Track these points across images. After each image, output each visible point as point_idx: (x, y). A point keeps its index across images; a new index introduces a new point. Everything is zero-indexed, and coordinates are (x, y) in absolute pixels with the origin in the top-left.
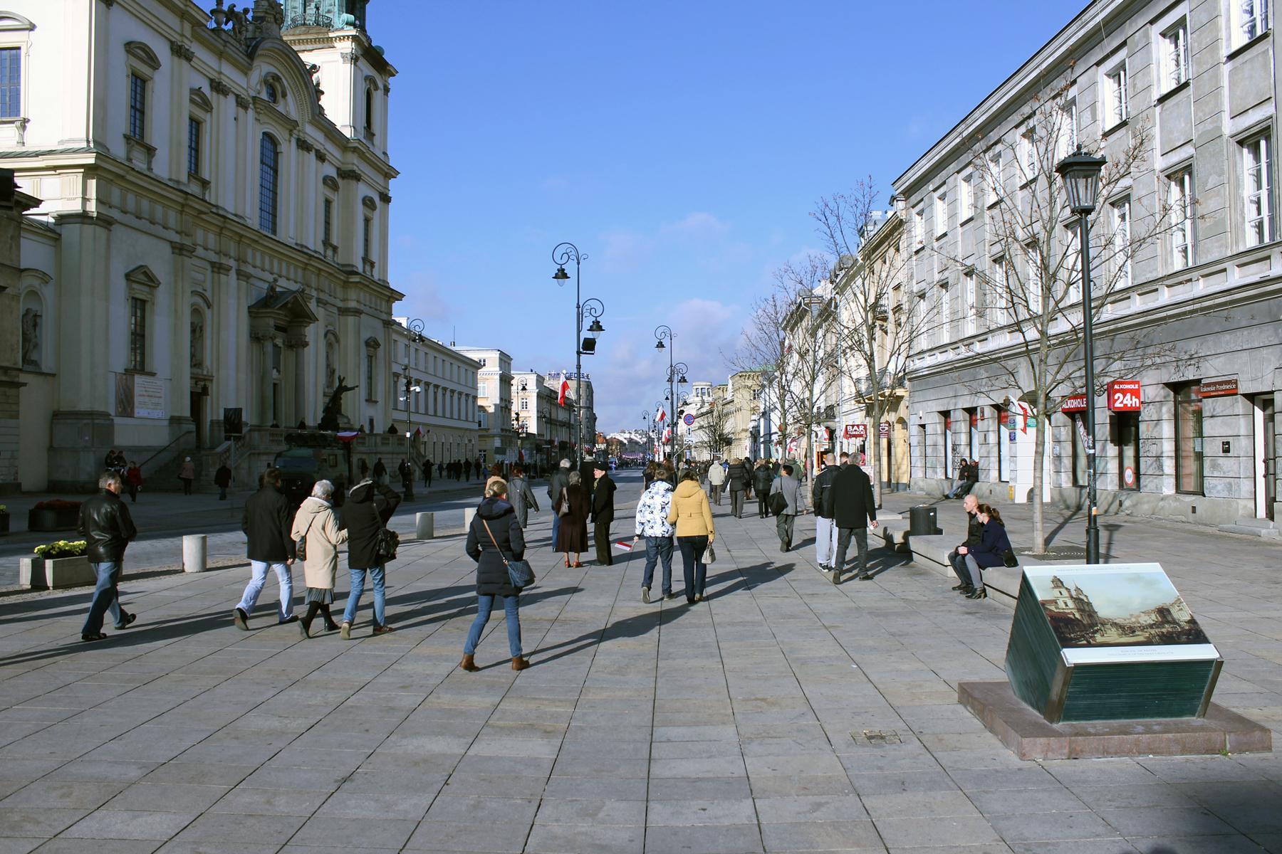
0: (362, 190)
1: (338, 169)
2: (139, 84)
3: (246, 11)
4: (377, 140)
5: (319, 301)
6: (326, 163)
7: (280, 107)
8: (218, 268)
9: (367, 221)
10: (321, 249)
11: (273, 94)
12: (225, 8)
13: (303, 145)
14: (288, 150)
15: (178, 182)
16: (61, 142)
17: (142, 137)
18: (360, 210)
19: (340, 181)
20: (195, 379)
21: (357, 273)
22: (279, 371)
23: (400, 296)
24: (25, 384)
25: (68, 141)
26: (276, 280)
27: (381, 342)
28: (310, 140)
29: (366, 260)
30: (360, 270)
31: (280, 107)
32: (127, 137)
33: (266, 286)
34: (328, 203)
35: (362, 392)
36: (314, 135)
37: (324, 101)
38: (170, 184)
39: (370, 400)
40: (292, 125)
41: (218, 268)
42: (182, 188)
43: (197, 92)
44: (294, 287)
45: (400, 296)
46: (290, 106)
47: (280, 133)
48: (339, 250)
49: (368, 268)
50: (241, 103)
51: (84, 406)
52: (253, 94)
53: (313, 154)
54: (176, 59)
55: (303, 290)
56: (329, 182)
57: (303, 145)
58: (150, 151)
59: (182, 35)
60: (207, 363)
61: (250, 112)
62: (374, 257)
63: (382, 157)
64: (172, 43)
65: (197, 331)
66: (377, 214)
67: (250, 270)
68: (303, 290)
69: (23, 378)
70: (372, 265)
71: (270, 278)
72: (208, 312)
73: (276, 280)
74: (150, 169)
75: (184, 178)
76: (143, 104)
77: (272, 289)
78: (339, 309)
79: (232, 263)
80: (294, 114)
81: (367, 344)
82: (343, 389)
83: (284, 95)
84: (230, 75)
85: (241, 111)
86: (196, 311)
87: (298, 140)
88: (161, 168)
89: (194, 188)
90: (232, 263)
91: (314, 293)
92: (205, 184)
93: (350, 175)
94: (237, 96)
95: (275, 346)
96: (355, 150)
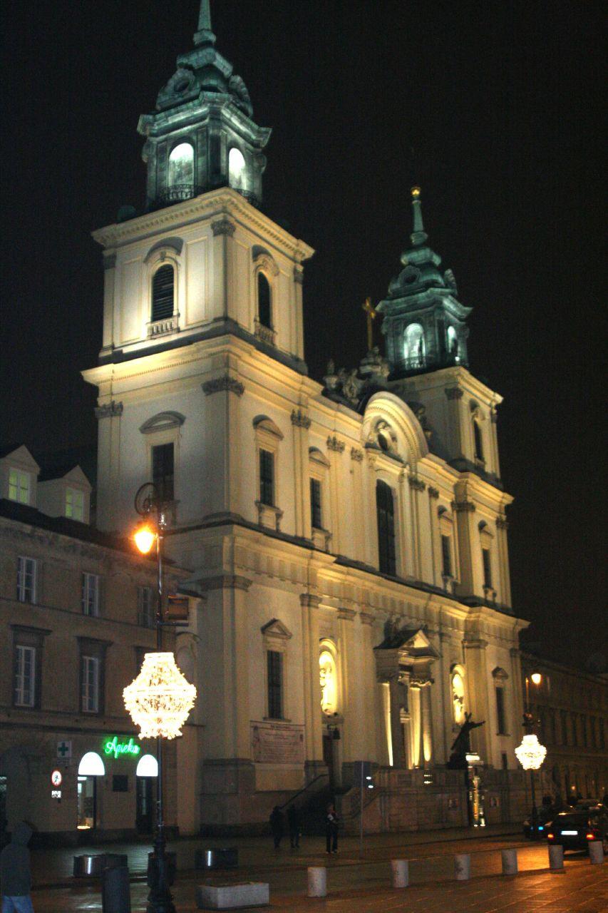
16: (207, 518)
51: (229, 755)
53: (426, 493)
54: (297, 429)
57: (416, 484)
61: (365, 462)
90: (355, 607)
94: (353, 451)
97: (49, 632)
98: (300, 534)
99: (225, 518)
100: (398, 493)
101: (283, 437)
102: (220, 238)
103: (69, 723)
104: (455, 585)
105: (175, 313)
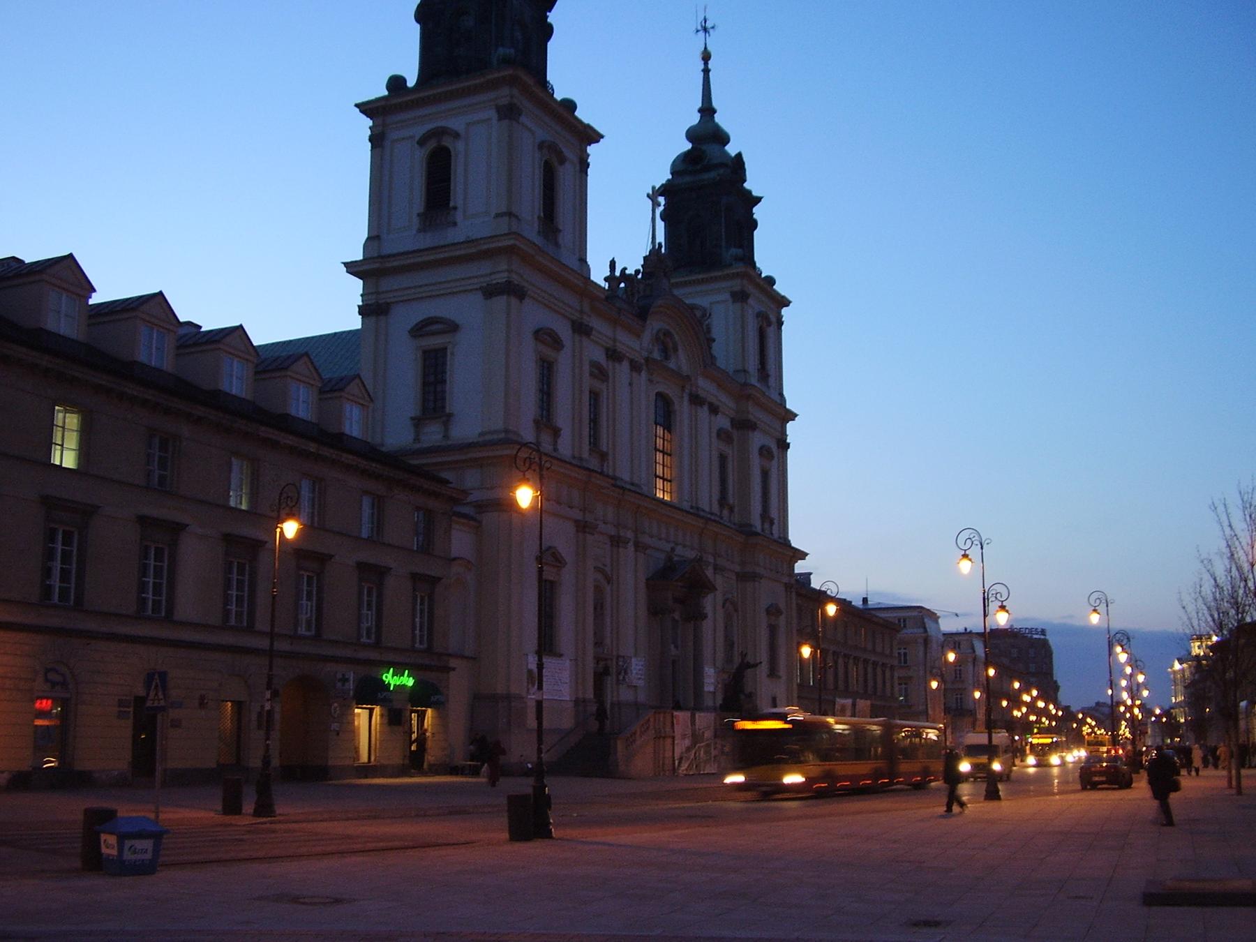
0: (757, 440)
1: (732, 420)
2: (547, 370)
3: (637, 272)
4: (772, 381)
5: (716, 568)
6: (720, 415)
7: (672, 364)
8: (616, 541)
9: (765, 475)
10: (716, 508)
11: (665, 352)
12: (618, 273)
13: (696, 400)
14: (683, 409)
15: (581, 459)
16: (481, 434)
17: (549, 420)
18: (756, 462)
19: (735, 434)
20: (598, 660)
21: (757, 534)
22: (676, 647)
23: (803, 555)
24: (454, 669)
25: (490, 433)
26: (673, 549)
27: (782, 606)
28: (702, 394)
29: (765, 515)
30: (759, 529)
31: (672, 364)
32: (536, 422)
33: (663, 556)
34: (723, 459)
35: (764, 668)
36: (705, 386)
37: (717, 349)
38: (574, 462)
39: (773, 673)
40: (683, 380)
41: (616, 541)
42: (585, 464)
43: (595, 365)
44: (690, 554)
45: (803, 555)
46: (682, 361)
47: (671, 391)
48: (736, 510)
49: (767, 526)
50: (635, 367)
52: (645, 354)
53: (706, 408)
54: (577, 337)
55: (701, 558)
56: (722, 435)
57: (696, 400)
58: (556, 432)
59: (581, 312)
60: (608, 641)
61: (644, 374)
62: (774, 513)
63: (777, 398)
64: (573, 322)
65: (599, 607)
66: (775, 462)
67: (646, 539)
68: (701, 558)
69: (453, 663)
70: (772, 523)
71: (668, 547)
72: (608, 588)
73: (673, 549)
74: (555, 450)
75: (586, 455)
76: (549, 387)
77: (669, 559)
78: (737, 574)
79: (630, 534)
80: (685, 369)
81: (768, 611)
82: (745, 666)
83: (676, 350)
84: (626, 342)
85: (634, 374)
86: (598, 589)
87: (691, 395)
88: (565, 447)
89: (594, 463)
90: (630, 534)
91: (711, 560)
92: (603, 456)
93: (744, 425)
94: (632, 362)
95: (674, 619)
96: (749, 397)
97: (331, 556)
98: (577, 455)
99: (502, 436)
100: (677, 407)
101: (563, 346)
102: (506, 122)
103: (348, 653)
104: (731, 510)
105: (452, 204)
